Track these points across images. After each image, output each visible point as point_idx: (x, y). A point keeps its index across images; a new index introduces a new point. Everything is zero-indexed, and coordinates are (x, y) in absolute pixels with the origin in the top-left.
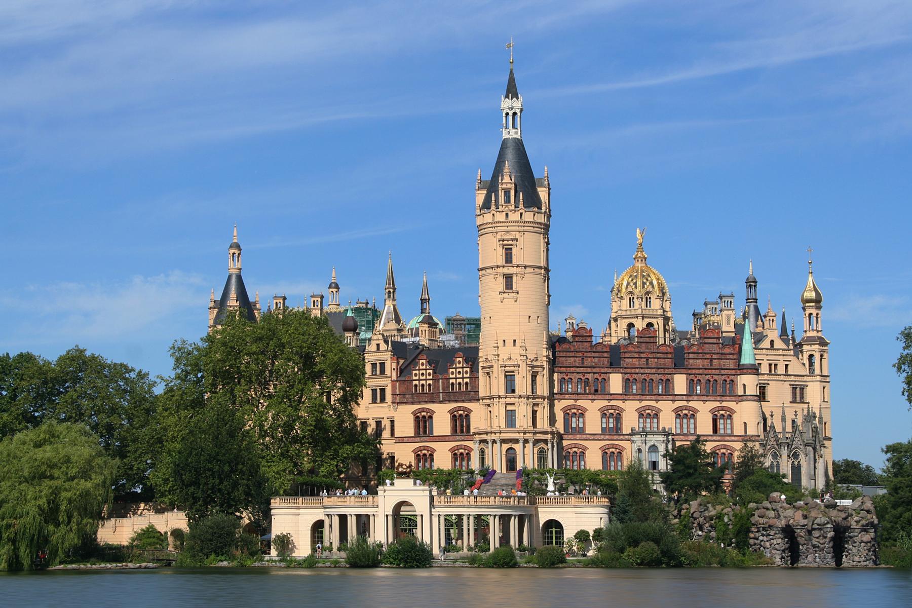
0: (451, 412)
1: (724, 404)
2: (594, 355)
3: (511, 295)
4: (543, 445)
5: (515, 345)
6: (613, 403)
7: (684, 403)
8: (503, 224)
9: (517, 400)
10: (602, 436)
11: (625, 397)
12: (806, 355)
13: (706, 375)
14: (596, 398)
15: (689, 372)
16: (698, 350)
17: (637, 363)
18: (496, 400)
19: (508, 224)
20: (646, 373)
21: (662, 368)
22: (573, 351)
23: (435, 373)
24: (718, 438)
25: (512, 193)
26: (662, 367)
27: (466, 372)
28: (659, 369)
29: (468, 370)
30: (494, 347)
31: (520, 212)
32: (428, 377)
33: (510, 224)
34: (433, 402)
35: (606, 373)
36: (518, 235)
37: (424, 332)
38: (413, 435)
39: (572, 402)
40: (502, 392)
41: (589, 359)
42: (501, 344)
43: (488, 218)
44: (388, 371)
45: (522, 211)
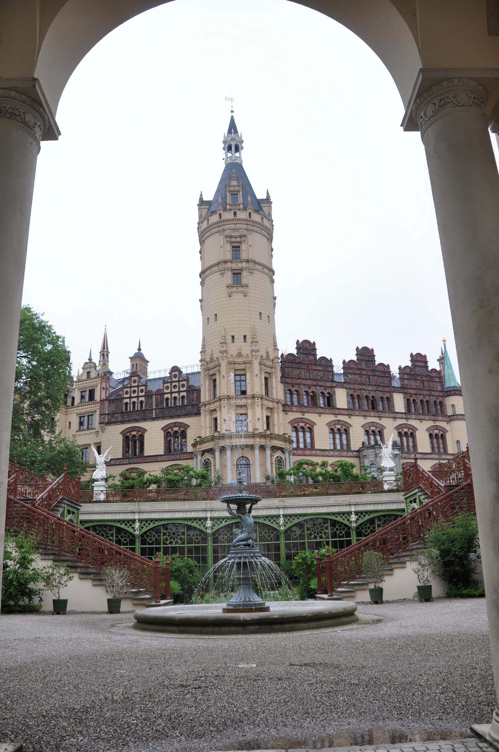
0: (165, 429)
1: (438, 423)
2: (318, 368)
3: (240, 289)
4: (279, 454)
5: (245, 341)
6: (340, 418)
7: (403, 421)
8: (232, 222)
9: (249, 401)
10: (332, 453)
13: (420, 394)
14: (323, 412)
16: (410, 371)
17: (359, 379)
18: (224, 402)
20: (369, 390)
21: (382, 386)
22: (298, 363)
23: (146, 388)
26: (382, 385)
27: (183, 386)
28: (379, 386)
29: (185, 383)
30: (221, 343)
31: (248, 212)
32: (140, 394)
33: (239, 222)
34: (145, 420)
35: (332, 387)
36: (245, 232)
37: (135, 366)
38: (121, 457)
39: (299, 415)
40: (232, 393)
41: (314, 372)
43: (215, 218)
44: (97, 397)
45: (251, 211)
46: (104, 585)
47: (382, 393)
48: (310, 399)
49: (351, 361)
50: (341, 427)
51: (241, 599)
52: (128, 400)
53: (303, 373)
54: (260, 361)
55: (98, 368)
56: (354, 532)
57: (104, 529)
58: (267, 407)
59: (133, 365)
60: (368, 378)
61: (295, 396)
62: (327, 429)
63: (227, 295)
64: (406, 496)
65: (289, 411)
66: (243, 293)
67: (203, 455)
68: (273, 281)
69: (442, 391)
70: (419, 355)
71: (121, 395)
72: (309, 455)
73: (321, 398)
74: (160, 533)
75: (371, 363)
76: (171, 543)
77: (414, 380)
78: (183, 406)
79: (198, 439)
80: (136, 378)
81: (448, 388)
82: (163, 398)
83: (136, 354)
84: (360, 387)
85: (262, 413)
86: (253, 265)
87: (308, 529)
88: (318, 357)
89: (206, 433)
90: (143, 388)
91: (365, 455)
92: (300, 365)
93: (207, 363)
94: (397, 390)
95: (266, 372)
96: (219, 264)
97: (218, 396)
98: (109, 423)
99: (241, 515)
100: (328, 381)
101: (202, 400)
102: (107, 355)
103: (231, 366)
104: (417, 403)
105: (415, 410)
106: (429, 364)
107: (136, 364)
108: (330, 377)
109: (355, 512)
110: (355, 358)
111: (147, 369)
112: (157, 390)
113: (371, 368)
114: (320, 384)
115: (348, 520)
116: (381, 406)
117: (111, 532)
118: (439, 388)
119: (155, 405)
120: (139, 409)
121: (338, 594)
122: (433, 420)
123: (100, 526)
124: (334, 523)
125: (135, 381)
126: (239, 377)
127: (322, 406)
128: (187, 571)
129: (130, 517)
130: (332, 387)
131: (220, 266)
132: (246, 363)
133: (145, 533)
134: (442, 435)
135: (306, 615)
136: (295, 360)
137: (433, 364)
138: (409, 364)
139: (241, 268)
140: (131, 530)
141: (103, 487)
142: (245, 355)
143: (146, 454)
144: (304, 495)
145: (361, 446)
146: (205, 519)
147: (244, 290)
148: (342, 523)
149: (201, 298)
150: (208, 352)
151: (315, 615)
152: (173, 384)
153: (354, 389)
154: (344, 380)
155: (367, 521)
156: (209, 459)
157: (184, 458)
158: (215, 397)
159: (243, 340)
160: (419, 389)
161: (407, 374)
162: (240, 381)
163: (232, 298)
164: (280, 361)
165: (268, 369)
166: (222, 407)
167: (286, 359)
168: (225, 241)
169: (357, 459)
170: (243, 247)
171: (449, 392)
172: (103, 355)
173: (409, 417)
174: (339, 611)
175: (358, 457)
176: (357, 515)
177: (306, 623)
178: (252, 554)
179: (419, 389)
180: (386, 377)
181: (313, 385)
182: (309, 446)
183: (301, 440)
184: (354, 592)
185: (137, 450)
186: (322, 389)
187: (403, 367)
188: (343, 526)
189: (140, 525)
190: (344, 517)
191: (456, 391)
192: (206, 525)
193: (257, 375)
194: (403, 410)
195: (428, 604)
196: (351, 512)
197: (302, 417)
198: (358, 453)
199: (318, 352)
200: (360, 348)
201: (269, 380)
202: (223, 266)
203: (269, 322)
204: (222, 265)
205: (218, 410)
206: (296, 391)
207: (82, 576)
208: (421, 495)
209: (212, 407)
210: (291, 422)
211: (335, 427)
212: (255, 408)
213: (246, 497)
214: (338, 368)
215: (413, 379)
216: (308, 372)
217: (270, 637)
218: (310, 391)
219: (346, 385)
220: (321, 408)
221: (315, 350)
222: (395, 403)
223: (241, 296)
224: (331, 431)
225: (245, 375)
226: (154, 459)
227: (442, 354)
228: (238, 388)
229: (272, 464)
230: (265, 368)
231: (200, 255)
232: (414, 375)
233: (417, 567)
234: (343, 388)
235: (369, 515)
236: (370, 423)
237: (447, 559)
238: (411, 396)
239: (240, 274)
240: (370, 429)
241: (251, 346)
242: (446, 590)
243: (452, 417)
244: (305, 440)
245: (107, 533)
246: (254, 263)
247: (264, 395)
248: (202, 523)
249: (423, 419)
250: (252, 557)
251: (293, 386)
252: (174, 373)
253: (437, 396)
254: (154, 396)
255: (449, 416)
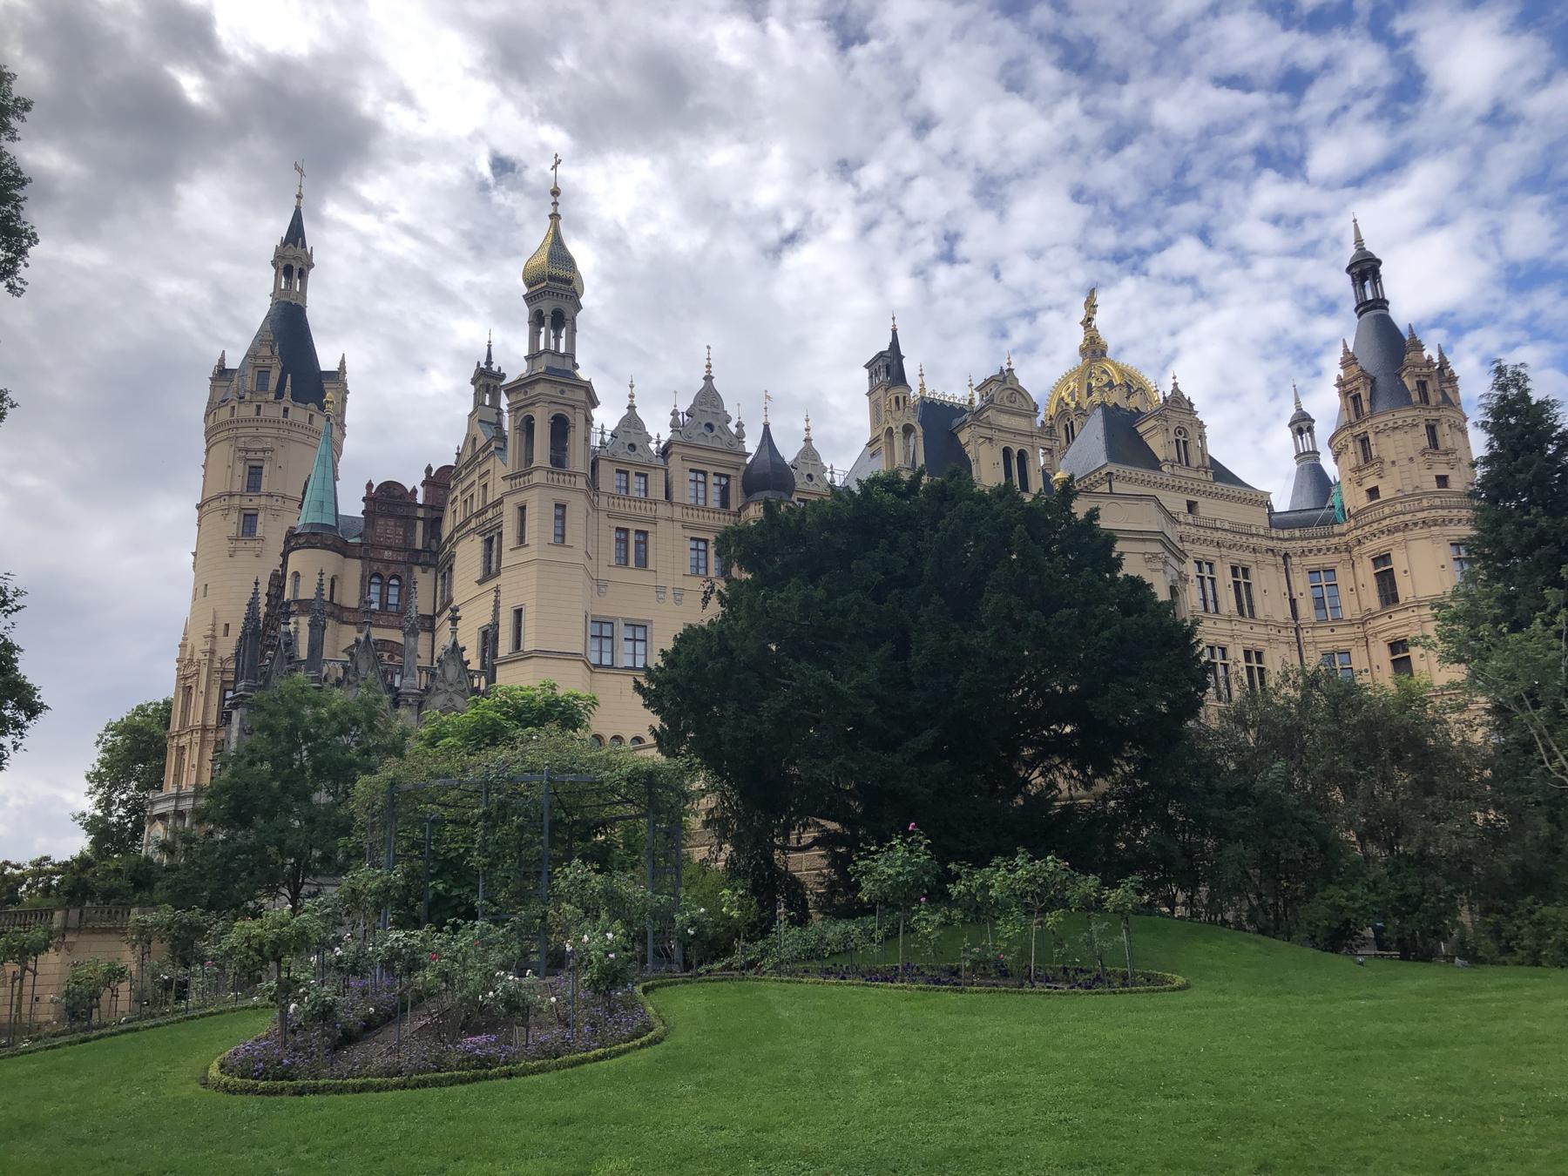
3: (252, 544)
19: (258, 424)
25: (275, 374)
33: (263, 424)
43: (224, 414)
63: (227, 553)
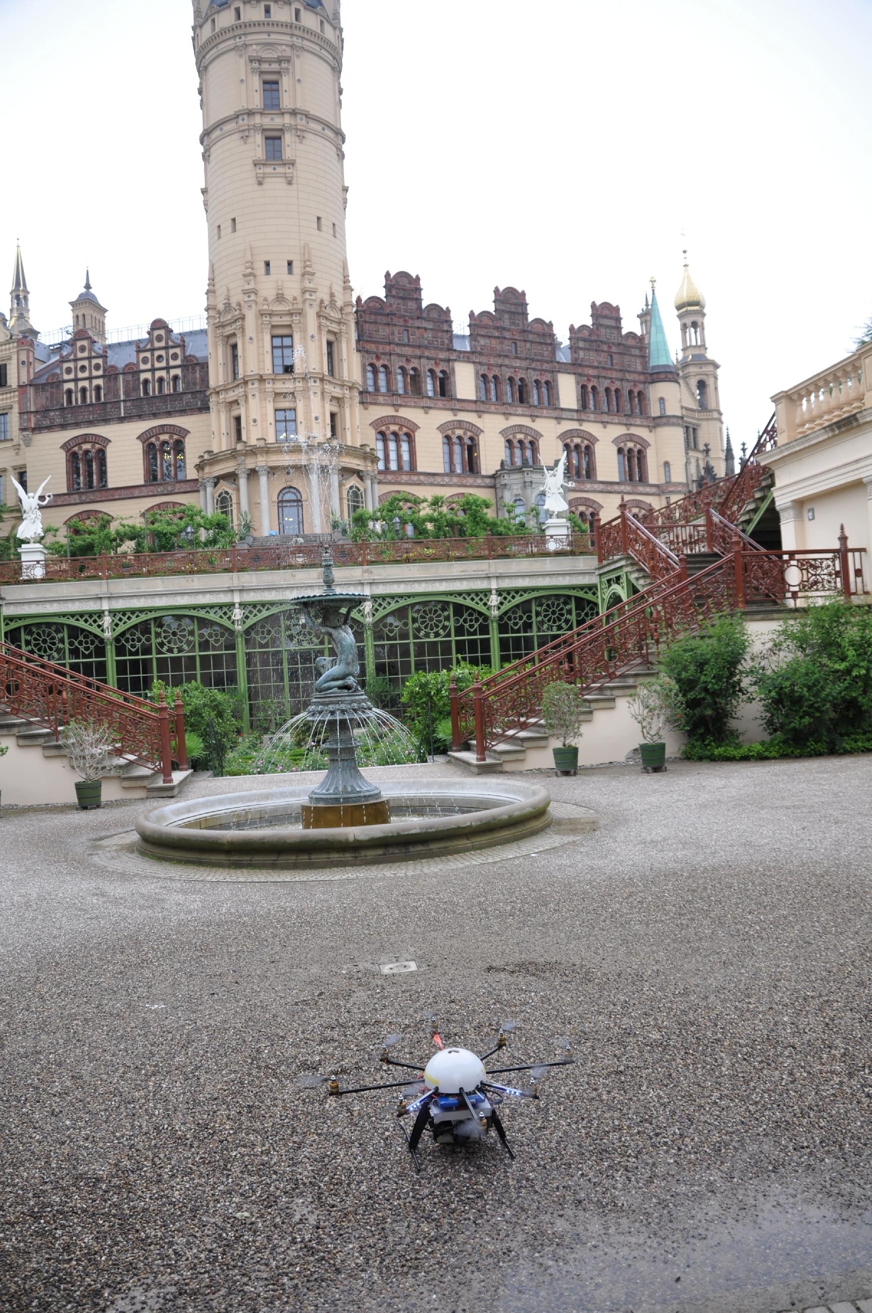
0: (144, 438)
1: (634, 430)
3: (280, 170)
4: (353, 481)
5: (290, 272)
6: (463, 416)
7: (574, 425)
9: (299, 385)
10: (447, 479)
11: (482, 407)
12: (693, 382)
13: (605, 378)
14: (432, 405)
15: (580, 370)
16: (590, 335)
18: (253, 388)
20: (515, 368)
21: (538, 361)
22: (388, 315)
23: (105, 362)
24: (628, 488)
26: (539, 358)
27: (175, 356)
28: (533, 360)
29: (178, 351)
30: (245, 276)
32: (95, 373)
34: (106, 421)
35: (449, 361)
37: (81, 318)
38: (65, 491)
39: (389, 411)
40: (268, 369)
41: (417, 332)
42: (260, 268)
46: (65, 756)
47: (539, 373)
48: (409, 380)
49: (485, 314)
50: (465, 434)
51: (337, 788)
52: (71, 385)
53: (396, 333)
54: (318, 310)
55: (10, 323)
56: (495, 625)
57: (47, 630)
58: (333, 397)
59: (77, 316)
60: (513, 345)
61: (382, 377)
62: (439, 438)
63: (254, 181)
64: (601, 571)
65: (371, 403)
66: (286, 177)
67: (216, 484)
68: (341, 156)
69: (644, 373)
70: (606, 305)
71: (57, 375)
72: (406, 484)
73: (429, 381)
74: (150, 633)
75: (520, 317)
76: (170, 650)
77: (596, 351)
78: (176, 396)
79: (206, 457)
80: (85, 343)
81: (654, 367)
82: (139, 379)
83: (81, 295)
84: (500, 361)
85: (324, 407)
86: (304, 122)
87: (414, 620)
88: (424, 305)
89: (222, 443)
90: (100, 361)
91: (505, 485)
92: (392, 319)
93: (219, 313)
94: (565, 368)
95: (329, 332)
96: (237, 117)
97: (240, 376)
98: (38, 429)
99: (330, 630)
100: (441, 350)
101: (212, 383)
102: (26, 298)
103: (264, 319)
104: (598, 393)
105: (595, 406)
106: (623, 323)
107: (84, 315)
108: (446, 341)
109: (497, 590)
110: (491, 308)
111: (103, 324)
112: (127, 366)
113: (521, 327)
114: (427, 353)
115: (485, 604)
116: (536, 397)
117: (60, 635)
118: (639, 368)
119: (126, 393)
120: (94, 401)
121: (492, 754)
122: (626, 425)
123: (39, 625)
124: (459, 609)
125: (83, 349)
126: (279, 340)
127: (430, 394)
128: (213, 714)
129: (92, 606)
130: (449, 361)
131: (241, 122)
132: (292, 314)
133: (123, 634)
134: (640, 452)
135: (469, 824)
136: (382, 308)
137: (630, 324)
138: (589, 322)
139: (280, 127)
140: (97, 631)
141: (39, 554)
142: (290, 298)
143: (111, 485)
144: (408, 561)
145: (499, 468)
146: (231, 605)
147: (288, 171)
148: (474, 610)
149: (204, 187)
150: (221, 292)
151: (485, 823)
152: (157, 353)
153: (490, 366)
154: (471, 348)
155: (517, 606)
156: (227, 493)
157: (183, 490)
158: (235, 378)
159: (286, 269)
160: (604, 368)
161: (584, 340)
162: (282, 347)
163: (265, 186)
164: (354, 309)
165: (334, 325)
166: (250, 396)
167: (365, 308)
168: (250, 71)
169: (493, 490)
170: (285, 82)
171: (655, 376)
172: (18, 297)
173: (584, 417)
174: (525, 811)
175: (494, 487)
176: (500, 595)
177: (468, 839)
178: (356, 705)
179: (604, 368)
180: (546, 344)
181: (415, 357)
182: (406, 467)
183: (393, 456)
184: (523, 751)
185: (95, 477)
186: (430, 365)
187: (576, 326)
188: (475, 615)
189: (113, 621)
190: (477, 599)
191: (668, 374)
192: (233, 617)
193: (312, 337)
194: (574, 406)
195: (657, 776)
196: (490, 591)
197: (395, 414)
198: (492, 480)
199: (424, 294)
200: (501, 289)
201: (335, 346)
202: (246, 121)
203: (335, 236)
204: (243, 120)
205: (242, 402)
206: (384, 366)
207: (22, 742)
208: (631, 572)
209: (231, 396)
210: (374, 424)
211: (453, 433)
212: (309, 398)
213: (341, 597)
214: (460, 326)
215: (592, 350)
216: (405, 333)
217: (410, 873)
218: (409, 367)
219: (473, 358)
220: (429, 398)
221: (418, 290)
222: (561, 393)
223: (280, 183)
224: (446, 441)
225: (291, 336)
226: (127, 493)
227: (647, 305)
228: (278, 362)
229: (341, 499)
230: (328, 323)
231: (200, 97)
232: (596, 341)
233: (641, 711)
234: (469, 362)
235: (521, 595)
236: (515, 426)
237: (691, 695)
238: (589, 380)
239: (279, 138)
240: (514, 437)
241: (302, 281)
242: (683, 748)
243: (658, 421)
244: (399, 457)
245: (54, 638)
246: (306, 116)
247: (327, 373)
248: (225, 613)
249: (607, 422)
250: (355, 711)
251: (378, 358)
252: (156, 333)
253: (635, 381)
254: (121, 377)
255: (654, 418)
